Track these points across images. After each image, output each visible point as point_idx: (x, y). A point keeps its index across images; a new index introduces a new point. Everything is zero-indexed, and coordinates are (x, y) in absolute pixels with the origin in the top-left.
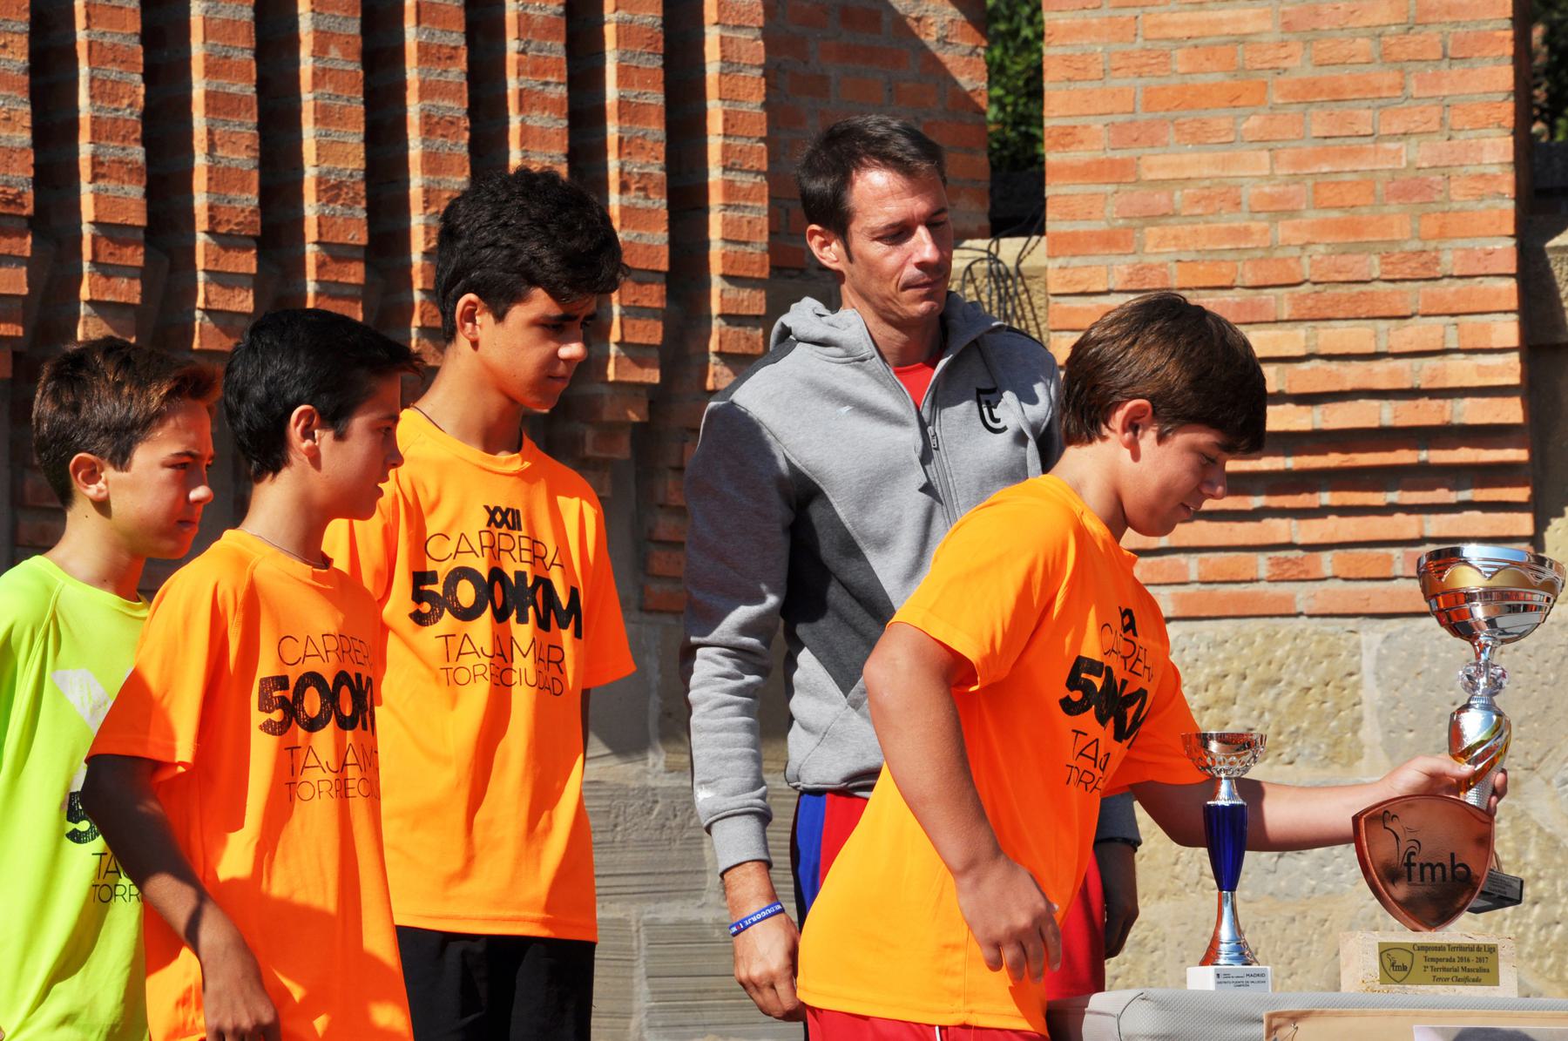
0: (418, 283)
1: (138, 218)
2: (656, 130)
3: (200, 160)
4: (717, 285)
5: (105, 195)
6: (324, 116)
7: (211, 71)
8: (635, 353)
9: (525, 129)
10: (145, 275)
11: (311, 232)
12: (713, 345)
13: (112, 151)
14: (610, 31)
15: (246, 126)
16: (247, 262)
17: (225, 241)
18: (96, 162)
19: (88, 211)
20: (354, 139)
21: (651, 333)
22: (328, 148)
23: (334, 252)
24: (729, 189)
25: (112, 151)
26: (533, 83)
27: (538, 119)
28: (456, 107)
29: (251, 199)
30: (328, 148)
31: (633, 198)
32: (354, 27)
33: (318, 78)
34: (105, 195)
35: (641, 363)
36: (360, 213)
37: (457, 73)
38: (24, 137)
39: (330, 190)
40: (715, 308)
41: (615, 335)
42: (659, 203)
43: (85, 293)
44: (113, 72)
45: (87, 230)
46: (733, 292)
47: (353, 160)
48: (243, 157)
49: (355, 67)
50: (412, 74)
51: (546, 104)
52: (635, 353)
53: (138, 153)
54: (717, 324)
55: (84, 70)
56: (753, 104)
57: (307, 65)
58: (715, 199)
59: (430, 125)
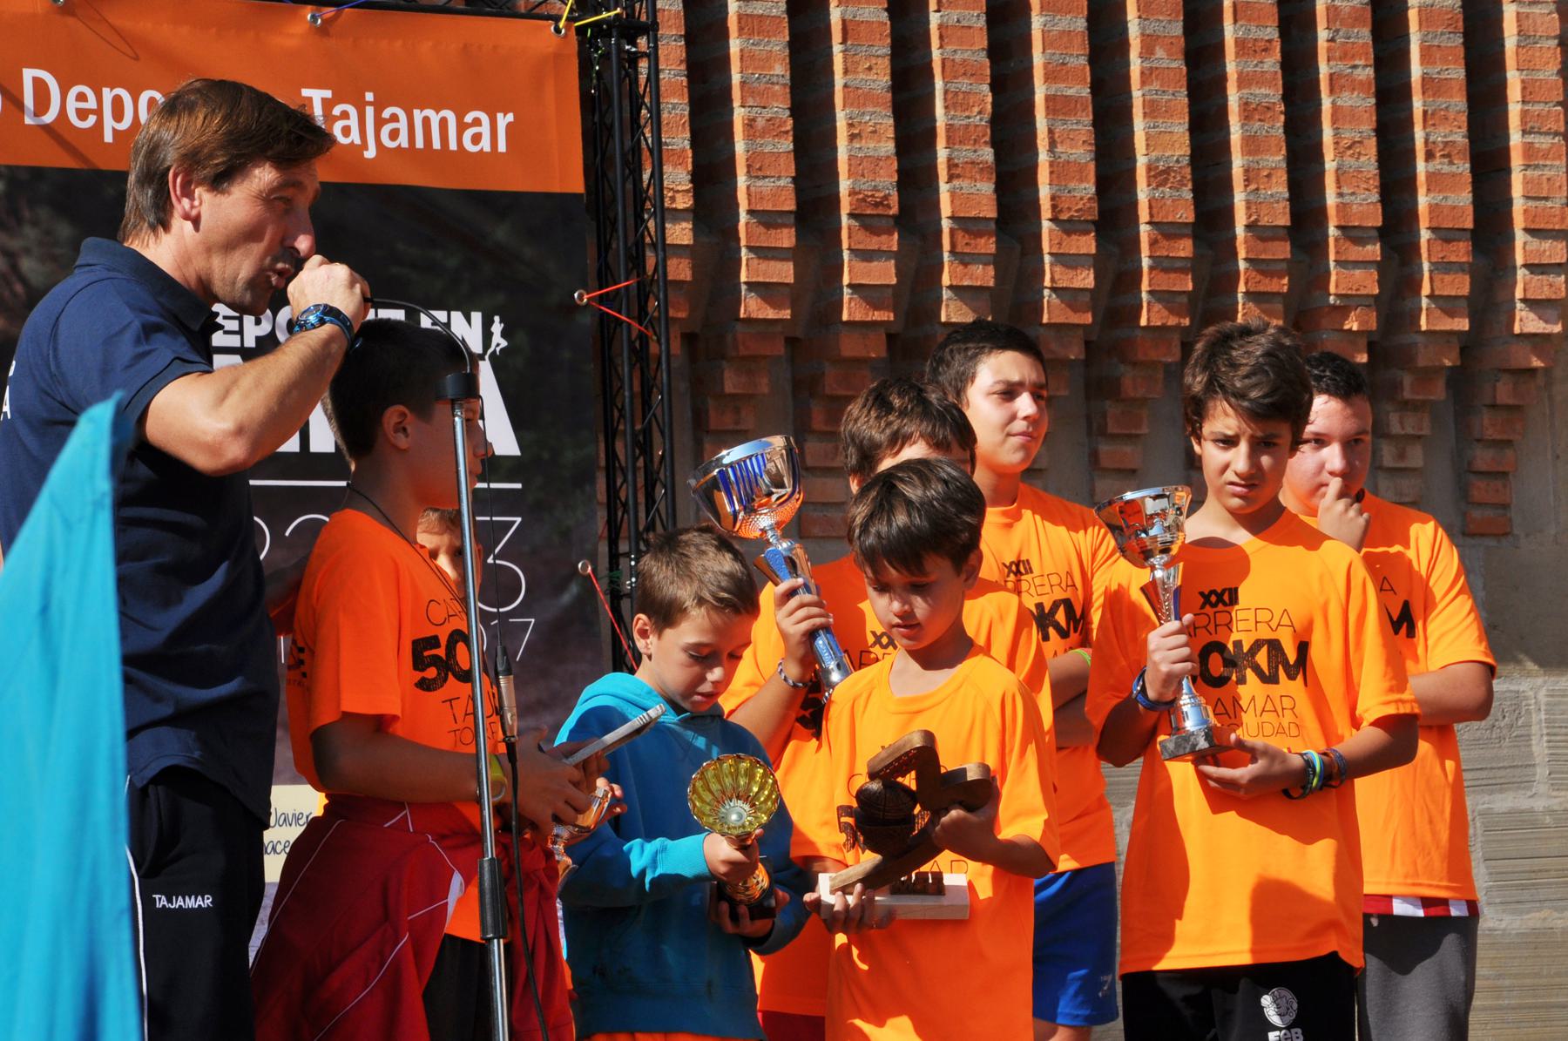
0: (1242, 253)
1: (991, 212)
2: (1458, 103)
3: (1043, 157)
4: (1520, 237)
5: (962, 192)
6: (1151, 110)
7: (1049, 77)
8: (1445, 304)
9: (1336, 109)
10: (998, 260)
11: (1144, 214)
12: (1519, 294)
13: (965, 154)
14: (1413, 16)
15: (1082, 125)
16: (1087, 244)
17: (1068, 226)
18: (951, 164)
19: (946, 209)
20: (1179, 129)
21: (1460, 285)
22: (1157, 137)
23: (1166, 231)
24: (1529, 150)
25: (965, 154)
26: (1341, 67)
27: (1348, 100)
28: (1272, 94)
29: (1088, 188)
30: (1157, 137)
31: (1438, 164)
32: (1177, 29)
33: (1146, 77)
34: (962, 192)
35: (1451, 314)
36: (1187, 194)
37: (1271, 63)
38: (888, 147)
39: (1159, 176)
40: (1519, 259)
41: (1426, 289)
42: (1463, 167)
43: (946, 280)
44: (964, 84)
45: (946, 225)
46: (1535, 244)
47: (1178, 145)
48: (1081, 152)
49: (1179, 64)
50: (1231, 67)
51: (1354, 86)
52: (1445, 304)
53: (988, 154)
54: (1521, 274)
55: (939, 84)
56: (1550, 72)
57: (1135, 65)
58: (1516, 161)
59: (1248, 112)
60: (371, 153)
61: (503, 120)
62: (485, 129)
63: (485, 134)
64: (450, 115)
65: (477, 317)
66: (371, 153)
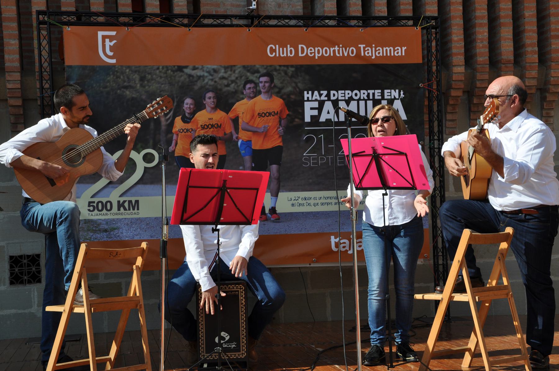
60: (374, 57)
61: (404, 49)
62: (400, 51)
63: (400, 52)
64: (392, 48)
65: (397, 91)
66: (374, 57)
